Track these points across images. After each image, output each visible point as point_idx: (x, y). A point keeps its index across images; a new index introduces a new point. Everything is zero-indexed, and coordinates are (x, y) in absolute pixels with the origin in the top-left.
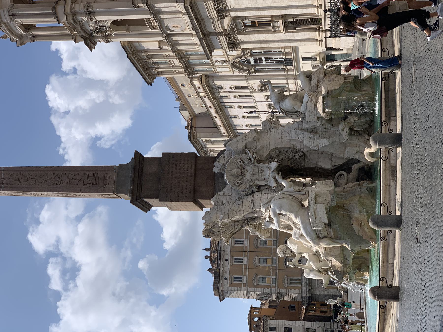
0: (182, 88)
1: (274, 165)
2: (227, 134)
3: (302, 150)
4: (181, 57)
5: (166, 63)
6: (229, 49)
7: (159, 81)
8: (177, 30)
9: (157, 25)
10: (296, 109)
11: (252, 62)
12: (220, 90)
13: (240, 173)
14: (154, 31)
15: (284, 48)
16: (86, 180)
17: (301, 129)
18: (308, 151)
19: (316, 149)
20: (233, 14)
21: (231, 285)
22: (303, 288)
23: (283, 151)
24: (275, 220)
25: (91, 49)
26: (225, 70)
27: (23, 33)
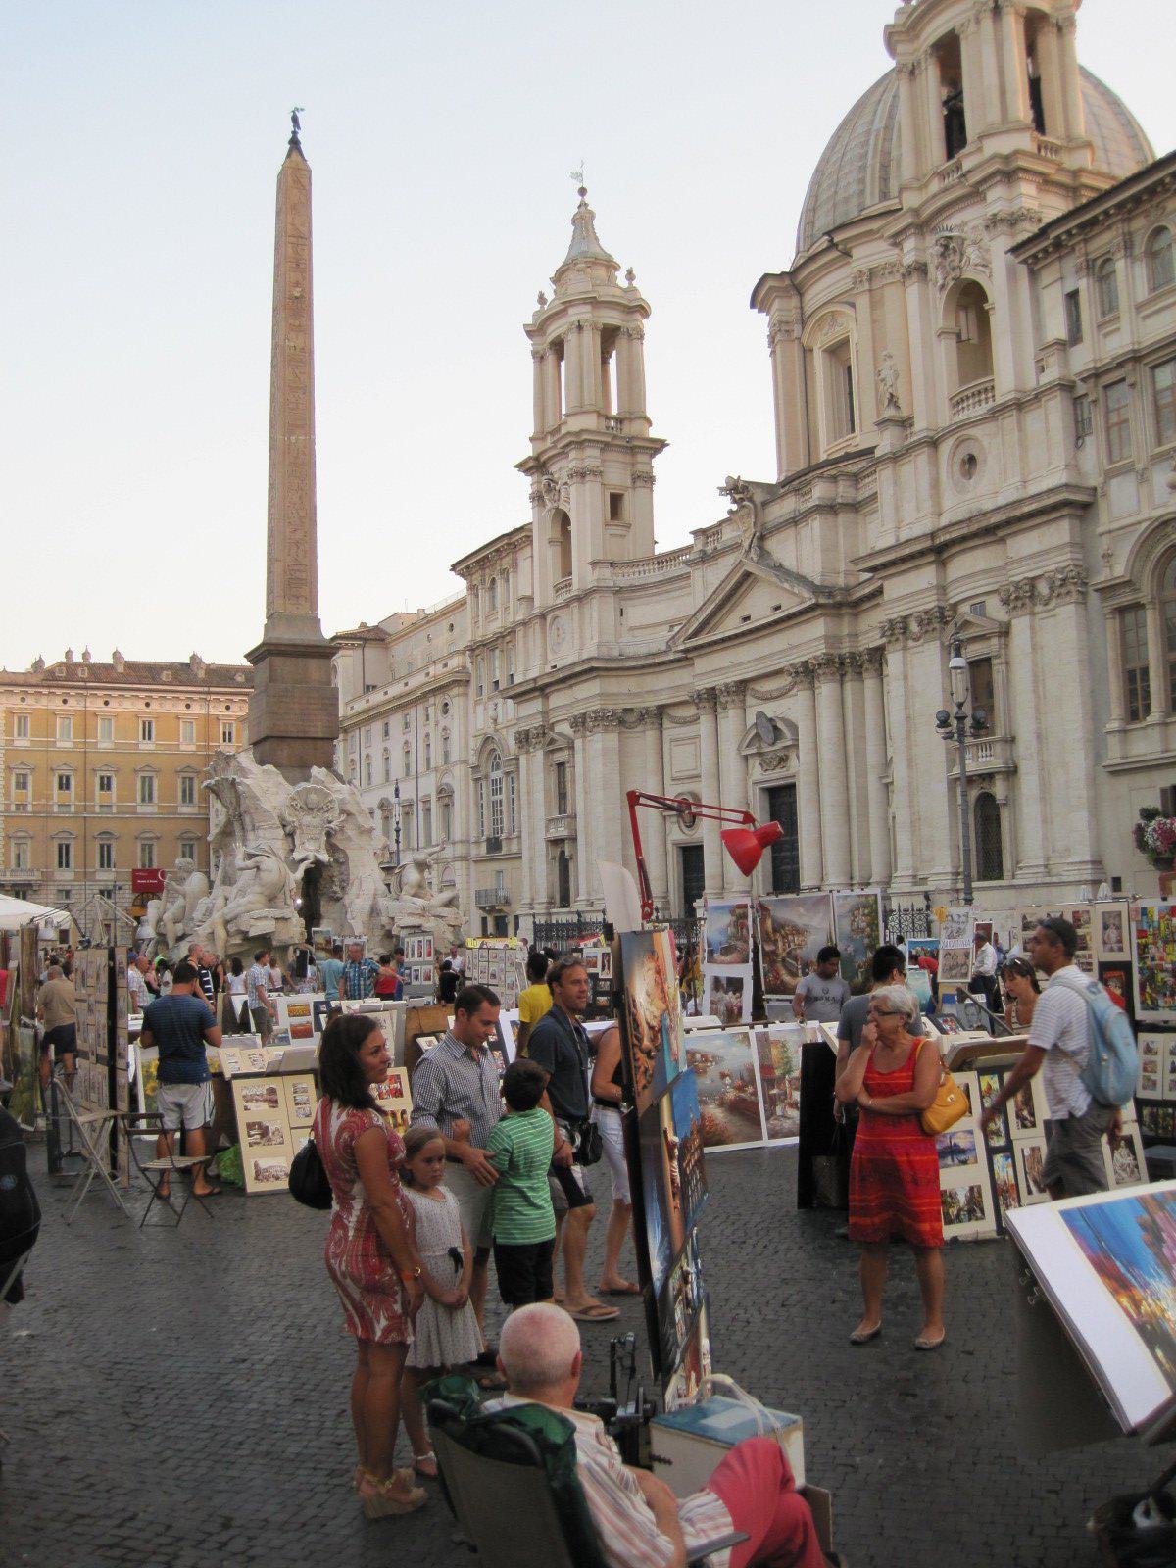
0: (445, 625)
1: (325, 857)
2: (350, 713)
3: (346, 897)
4: (503, 637)
5: (493, 607)
6: (519, 733)
7: (458, 587)
8: (551, 635)
9: (560, 600)
10: (405, 888)
11: (496, 775)
12: (440, 707)
13: (310, 806)
14: (551, 591)
15: (519, 837)
16: (295, 568)
17: (375, 894)
18: (344, 905)
19: (349, 916)
20: (578, 743)
21: (10, 712)
22: (8, 874)
23: (344, 867)
24: (249, 863)
25: (520, 466)
26: (481, 722)
27: (550, 339)
